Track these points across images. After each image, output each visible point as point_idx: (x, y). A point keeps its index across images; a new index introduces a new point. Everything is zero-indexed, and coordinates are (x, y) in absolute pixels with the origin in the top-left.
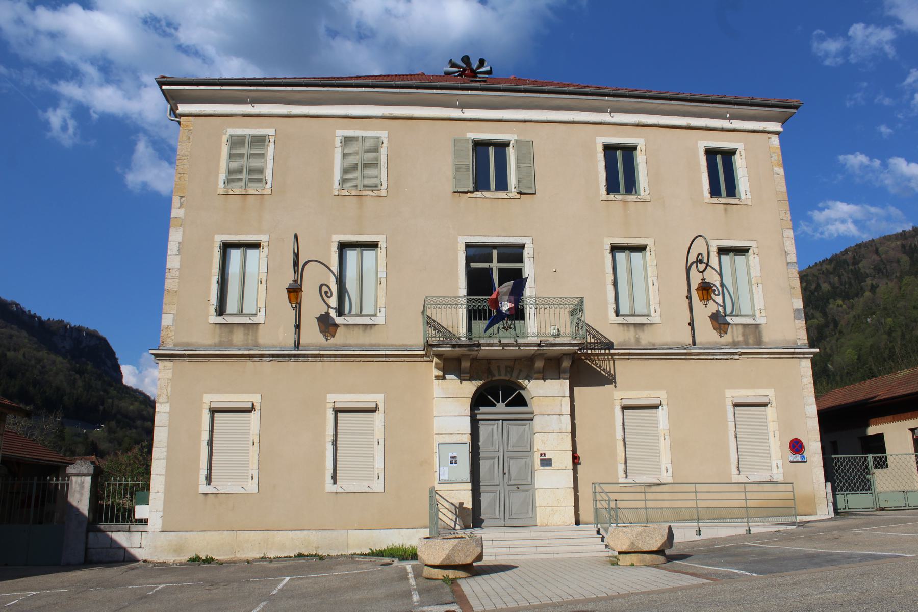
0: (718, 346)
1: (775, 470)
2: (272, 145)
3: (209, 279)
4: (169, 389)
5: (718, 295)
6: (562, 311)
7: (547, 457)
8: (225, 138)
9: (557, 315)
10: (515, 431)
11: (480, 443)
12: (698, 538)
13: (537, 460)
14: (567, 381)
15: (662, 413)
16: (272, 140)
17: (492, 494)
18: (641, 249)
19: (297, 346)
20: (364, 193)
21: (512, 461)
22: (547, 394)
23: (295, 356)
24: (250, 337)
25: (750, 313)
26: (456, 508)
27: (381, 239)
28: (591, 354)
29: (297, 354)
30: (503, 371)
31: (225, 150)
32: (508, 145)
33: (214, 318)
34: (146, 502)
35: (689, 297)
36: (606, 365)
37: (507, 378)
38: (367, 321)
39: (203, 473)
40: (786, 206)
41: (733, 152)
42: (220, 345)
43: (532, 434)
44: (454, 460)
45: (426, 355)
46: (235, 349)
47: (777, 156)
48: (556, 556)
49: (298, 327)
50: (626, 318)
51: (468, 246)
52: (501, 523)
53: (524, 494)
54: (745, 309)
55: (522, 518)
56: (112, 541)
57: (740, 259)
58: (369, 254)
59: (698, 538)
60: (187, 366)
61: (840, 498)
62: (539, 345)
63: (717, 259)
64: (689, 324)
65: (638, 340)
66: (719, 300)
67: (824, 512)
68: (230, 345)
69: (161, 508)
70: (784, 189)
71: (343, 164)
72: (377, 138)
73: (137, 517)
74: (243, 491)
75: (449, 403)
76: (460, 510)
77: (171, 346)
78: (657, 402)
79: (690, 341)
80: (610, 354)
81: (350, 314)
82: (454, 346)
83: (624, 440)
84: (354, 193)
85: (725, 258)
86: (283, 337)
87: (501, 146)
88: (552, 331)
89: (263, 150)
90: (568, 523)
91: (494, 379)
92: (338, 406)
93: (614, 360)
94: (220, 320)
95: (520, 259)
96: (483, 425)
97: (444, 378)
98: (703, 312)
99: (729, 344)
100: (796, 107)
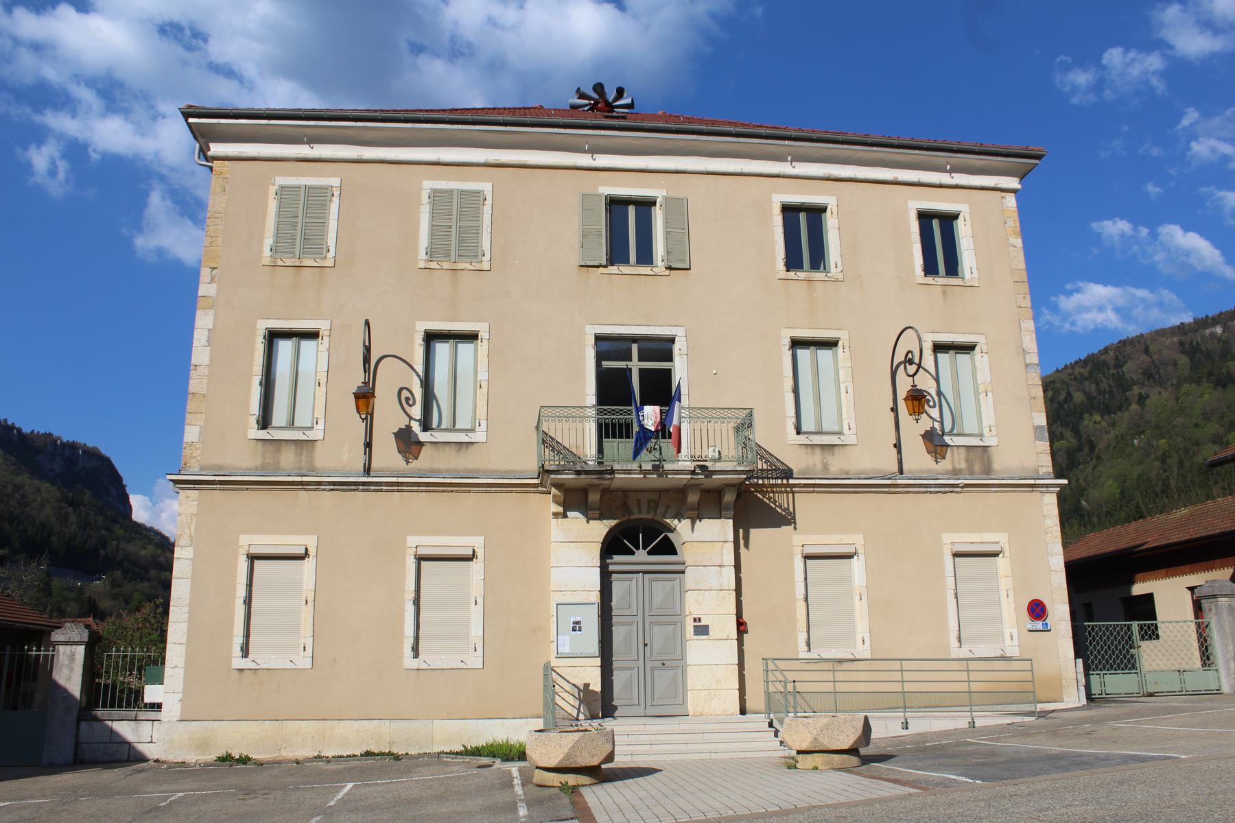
0: (933, 475)
1: (1008, 642)
2: (336, 199)
3: (249, 380)
4: (193, 528)
5: (934, 406)
8: (272, 190)
10: (660, 588)
12: (905, 732)
13: (690, 626)
15: (857, 564)
16: (337, 193)
18: (831, 344)
19: (367, 470)
20: (460, 266)
21: (655, 628)
22: (704, 540)
23: (364, 484)
24: (304, 458)
25: (977, 432)
27: (482, 328)
28: (763, 485)
29: (366, 482)
30: (644, 507)
31: (272, 205)
32: (654, 203)
33: (254, 433)
34: (159, 680)
35: (894, 410)
36: (783, 499)
37: (650, 517)
38: (462, 437)
39: (238, 641)
40: (1025, 288)
41: (955, 216)
42: (263, 469)
43: (683, 592)
44: (577, 627)
45: (541, 485)
46: (284, 475)
47: (1013, 222)
48: (714, 756)
49: (368, 445)
50: (811, 437)
51: (599, 338)
52: (641, 711)
53: (672, 672)
54: (969, 425)
55: (670, 707)
56: (112, 732)
57: (963, 358)
58: (465, 349)
59: (905, 732)
60: (218, 496)
61: (1094, 679)
62: (693, 472)
63: (932, 358)
64: (895, 446)
65: (825, 467)
66: (935, 413)
67: (1074, 697)
68: (277, 469)
69: (180, 689)
70: (1022, 266)
71: (433, 228)
72: (478, 192)
73: (147, 700)
74: (291, 666)
75: (571, 550)
76: (585, 694)
77: (196, 470)
78: (851, 550)
79: (896, 468)
80: (788, 485)
81: (439, 428)
82: (578, 473)
83: (806, 600)
84: (446, 265)
85: (942, 357)
87: (645, 206)
89: (324, 206)
90: (731, 711)
92: (421, 552)
93: (793, 493)
94: (263, 434)
95: (670, 358)
96: (617, 579)
97: (565, 516)
98: (914, 430)
99: (947, 473)
100: (1039, 157)
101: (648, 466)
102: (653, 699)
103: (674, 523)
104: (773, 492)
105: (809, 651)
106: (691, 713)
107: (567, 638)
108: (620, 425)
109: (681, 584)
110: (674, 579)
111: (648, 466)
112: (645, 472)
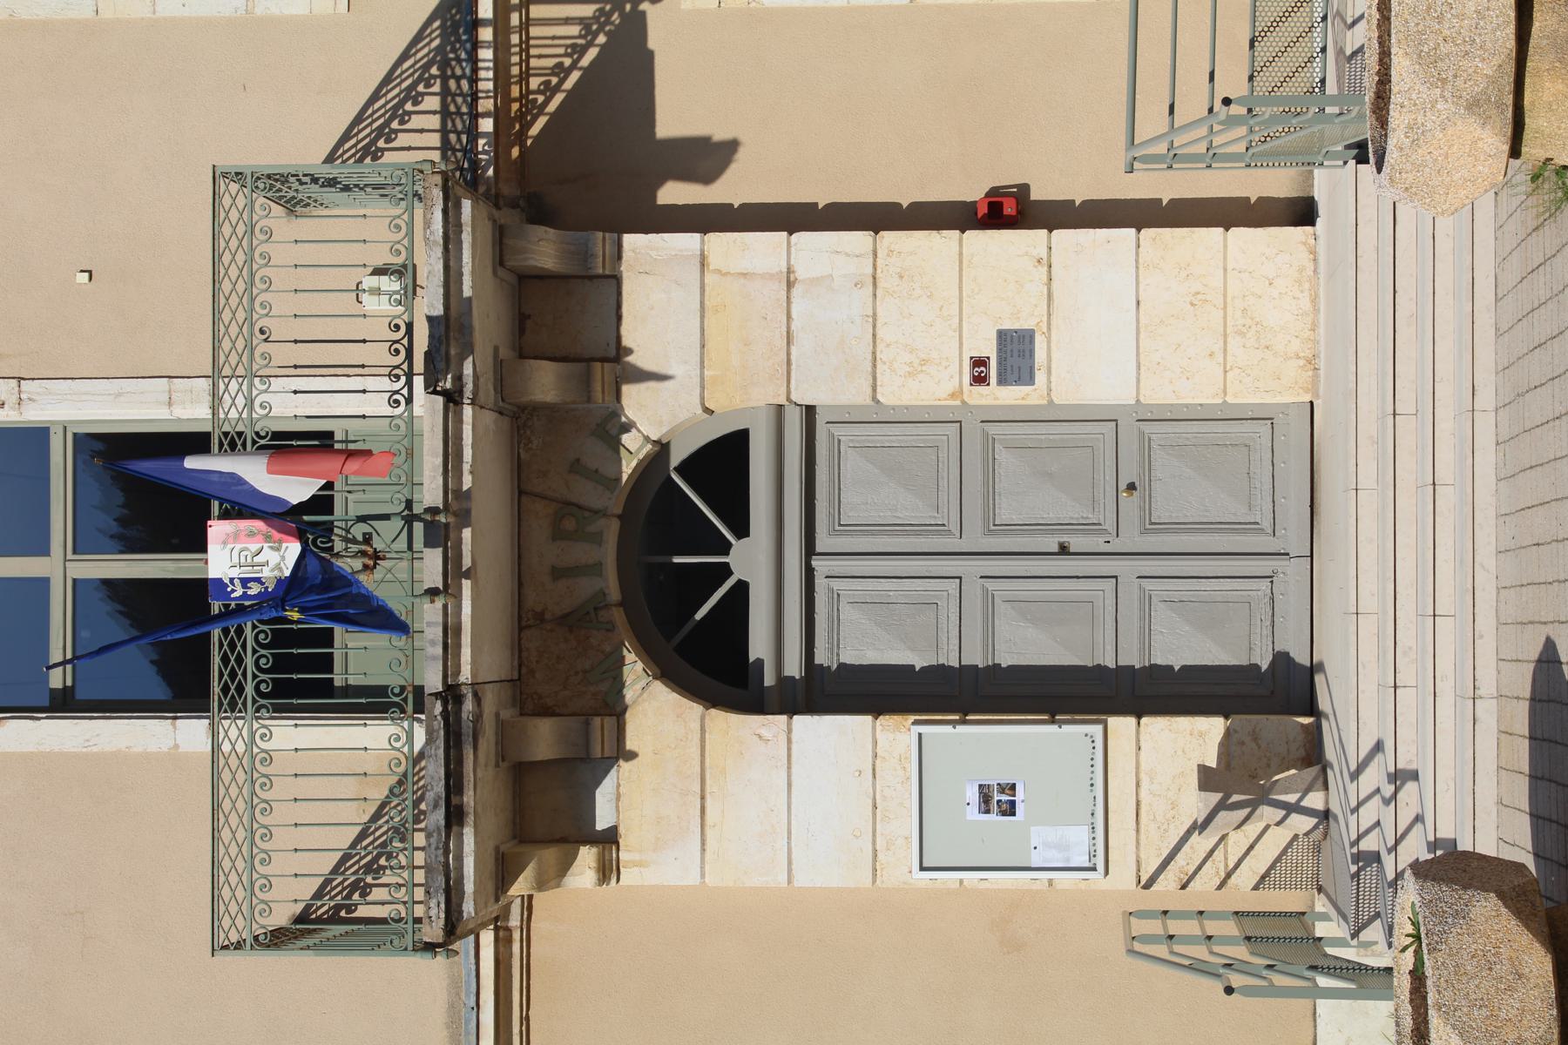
6: (281, 253)
7: (989, 350)
9: (308, 279)
10: (864, 494)
13: (998, 395)
14: (629, 240)
17: (1161, 613)
22: (699, 334)
28: (497, 115)
30: (580, 553)
37: (611, 531)
43: (879, 417)
44: (999, 800)
45: (500, 925)
48: (1486, 399)
53: (1159, 457)
55: (1284, 465)
62: (452, 399)
75: (723, 810)
76: (1233, 782)
82: (455, 817)
88: (381, 304)
90: (1304, 257)
91: (614, 594)
95: (37, 436)
96: (835, 646)
97: (610, 838)
101: (431, 565)
102: (1252, 527)
103: (634, 449)
104: (525, 76)
106: (1308, 398)
107: (1038, 835)
108: (280, 664)
109: (851, 419)
112: (453, 571)
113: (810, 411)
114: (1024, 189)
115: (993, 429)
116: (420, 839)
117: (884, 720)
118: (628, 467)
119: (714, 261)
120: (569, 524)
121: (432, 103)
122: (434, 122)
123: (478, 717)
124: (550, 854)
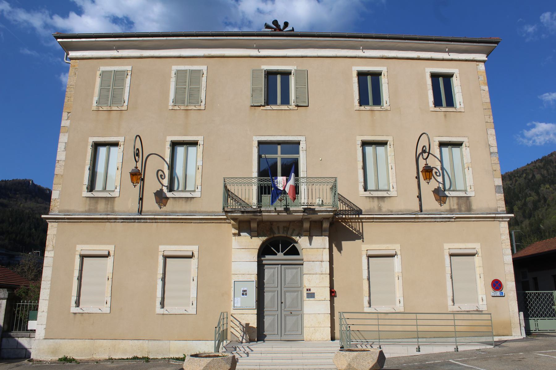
0: (439, 213)
1: (481, 302)
2: (129, 77)
3: (84, 167)
4: (54, 241)
5: (440, 176)
6: (325, 187)
8: (98, 73)
10: (290, 272)
11: (265, 281)
12: (418, 353)
14: (327, 238)
15: (397, 261)
16: (129, 74)
17: (272, 317)
18: (383, 144)
19: (140, 212)
20: (190, 108)
21: (287, 294)
23: (138, 219)
24: (109, 206)
25: (463, 189)
26: (243, 327)
27: (200, 139)
28: (345, 218)
29: (139, 218)
30: (281, 230)
31: (98, 80)
32: (290, 73)
33: (86, 194)
34: (35, 318)
35: (418, 178)
36: (357, 226)
37: (284, 235)
38: (188, 195)
39: (74, 299)
40: (490, 112)
41: (451, 75)
42: (89, 211)
44: (244, 293)
46: (101, 214)
47: (483, 77)
48: (305, 367)
49: (141, 199)
50: (372, 192)
51: (260, 143)
52: (279, 337)
54: (459, 185)
56: (18, 343)
57: (456, 150)
58: (192, 149)
59: (418, 353)
60: (67, 226)
61: (532, 322)
63: (438, 150)
64: (418, 197)
65: (380, 209)
66: (440, 179)
67: (518, 333)
68: (96, 211)
69: (45, 323)
70: (488, 100)
71: (176, 89)
72: (200, 71)
73: (29, 328)
74: (100, 312)
75: (243, 253)
76: (247, 328)
77: (57, 213)
78: (393, 252)
79: (418, 208)
80: (359, 218)
81: (178, 190)
82: (243, 212)
83: (369, 279)
84: (182, 108)
85: (445, 150)
86: (132, 206)
87: (286, 74)
88: (318, 201)
89: (123, 80)
90: (326, 339)
91: (275, 235)
92: (166, 253)
93: (362, 222)
94: (90, 194)
95: (298, 153)
96: (268, 268)
97: (239, 235)
98: (428, 188)
99: (447, 211)
100: (497, 43)
102: (285, 331)
103: (297, 238)
104: (351, 222)
105: (370, 306)
107: (239, 299)
108: (265, 187)
110: (297, 268)
111: (282, 209)
113: (302, 265)
114: (336, 296)
115: (300, 292)
116: (239, 207)
117: (256, 276)
118: (294, 237)
119: (324, 250)
120: (285, 229)
121: (347, 209)
122: (344, 209)
123: (257, 216)
124: (237, 226)
